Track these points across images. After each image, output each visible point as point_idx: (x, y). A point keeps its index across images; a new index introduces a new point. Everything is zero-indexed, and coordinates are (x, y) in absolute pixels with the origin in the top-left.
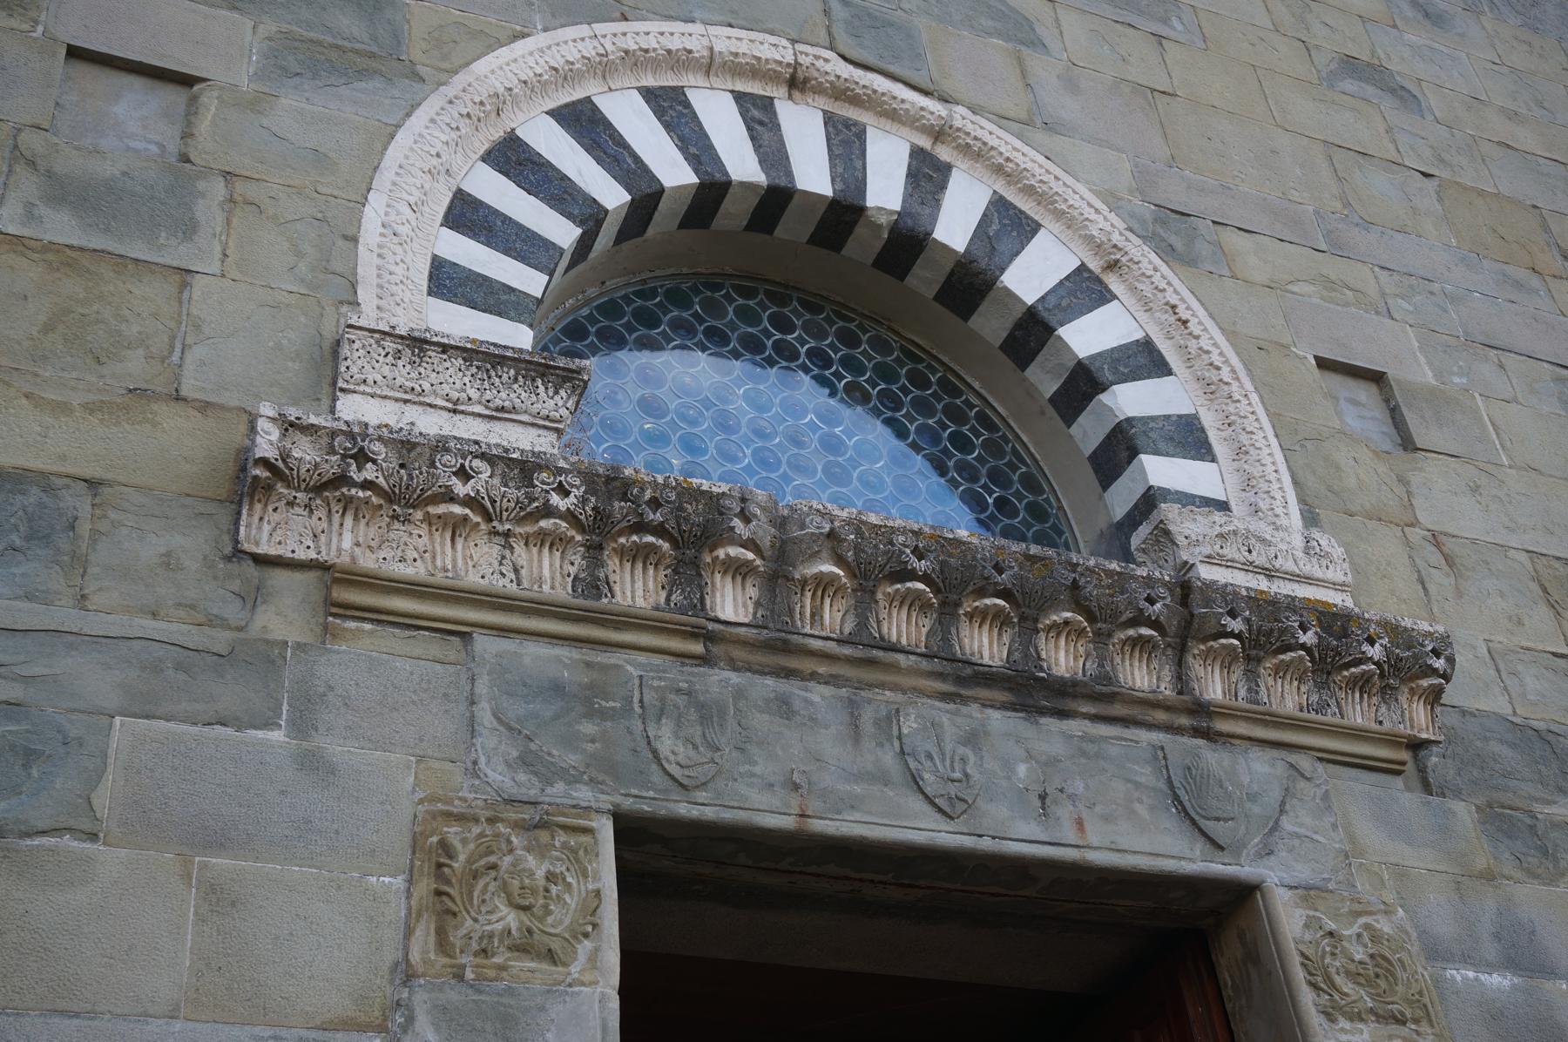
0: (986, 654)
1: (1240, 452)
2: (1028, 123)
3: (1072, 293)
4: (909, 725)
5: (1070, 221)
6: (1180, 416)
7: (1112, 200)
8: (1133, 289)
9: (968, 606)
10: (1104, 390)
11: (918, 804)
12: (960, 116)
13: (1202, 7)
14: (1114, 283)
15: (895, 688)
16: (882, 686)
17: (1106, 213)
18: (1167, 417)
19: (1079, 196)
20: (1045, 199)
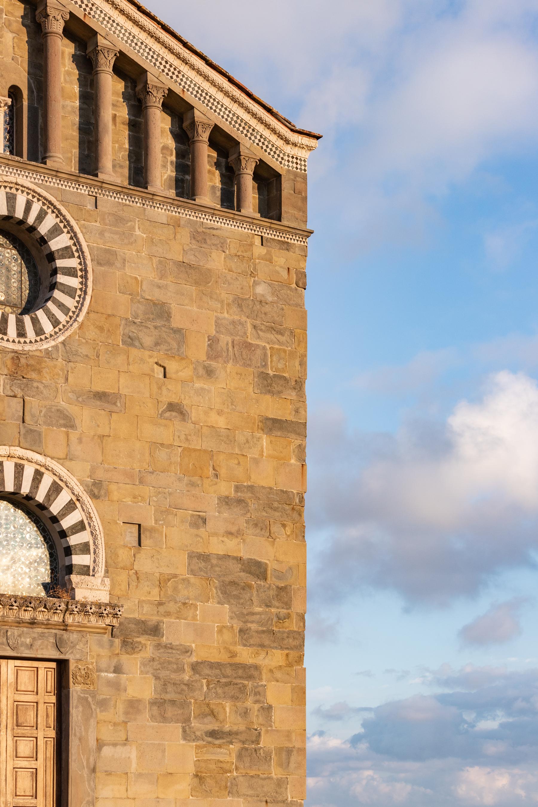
0: (26, 616)
1: (95, 553)
2: (66, 458)
3: (67, 510)
4: (9, 634)
5: (72, 490)
6: (84, 543)
7: (81, 482)
8: (82, 506)
9: (23, 608)
10: (68, 537)
11: (8, 648)
12: (49, 462)
13: (128, 394)
14: (78, 504)
15: (8, 626)
16: (5, 625)
17: (79, 486)
18: (81, 544)
19: (73, 482)
20: (66, 483)
